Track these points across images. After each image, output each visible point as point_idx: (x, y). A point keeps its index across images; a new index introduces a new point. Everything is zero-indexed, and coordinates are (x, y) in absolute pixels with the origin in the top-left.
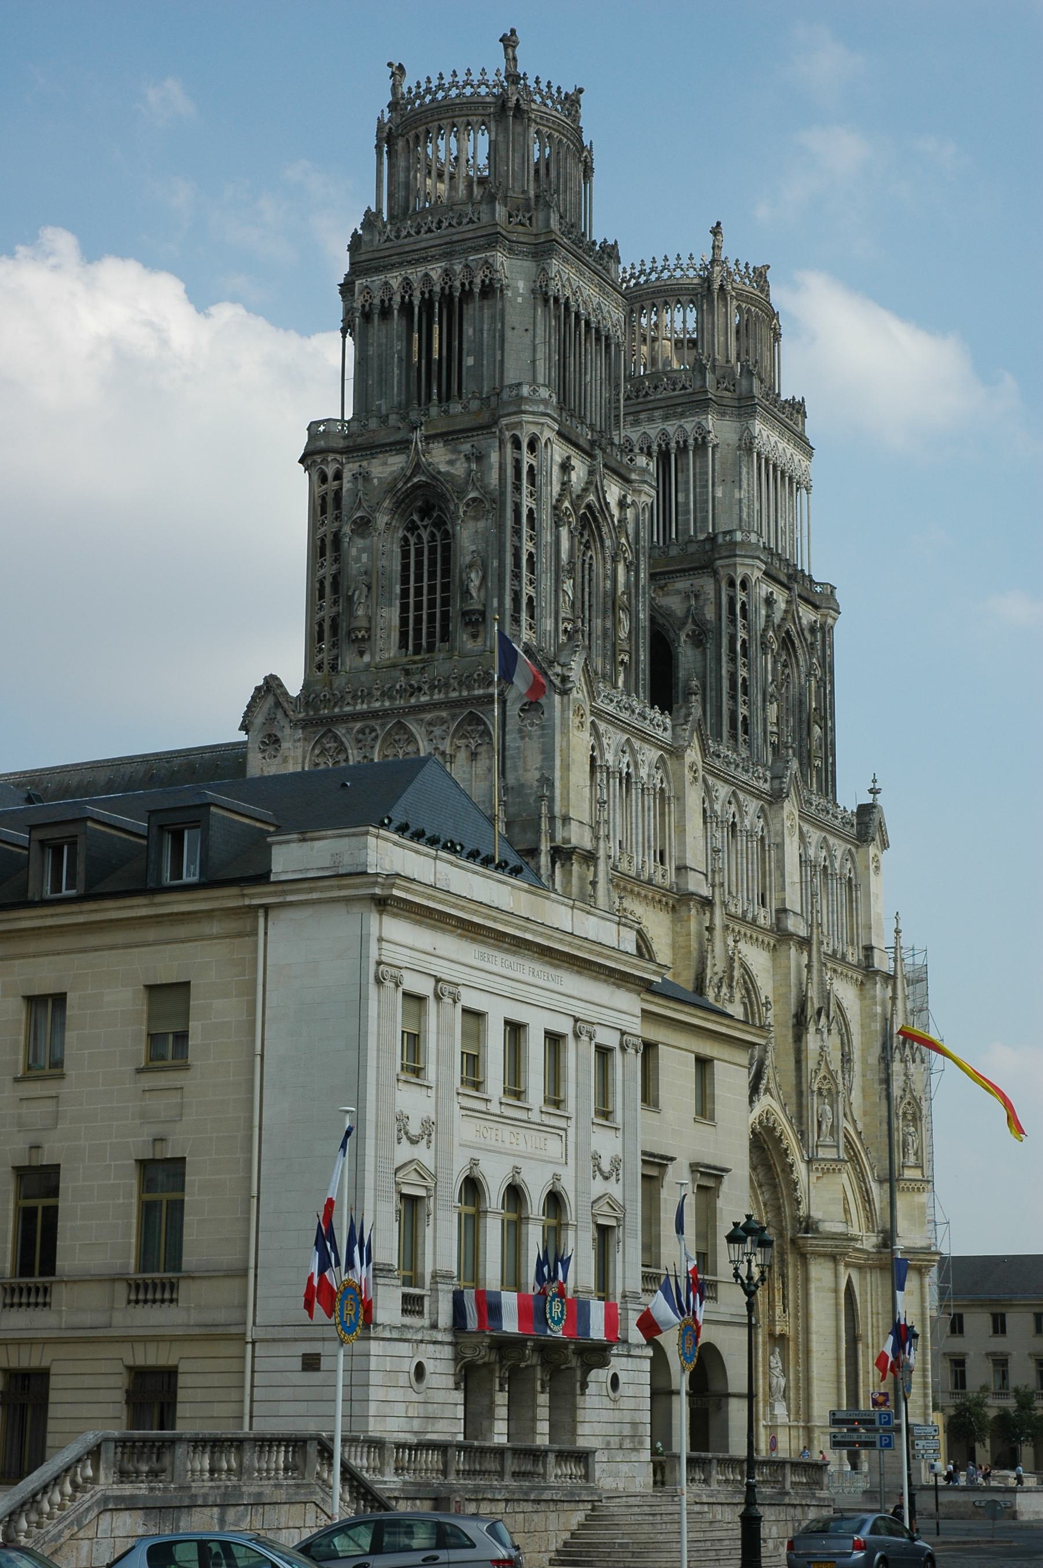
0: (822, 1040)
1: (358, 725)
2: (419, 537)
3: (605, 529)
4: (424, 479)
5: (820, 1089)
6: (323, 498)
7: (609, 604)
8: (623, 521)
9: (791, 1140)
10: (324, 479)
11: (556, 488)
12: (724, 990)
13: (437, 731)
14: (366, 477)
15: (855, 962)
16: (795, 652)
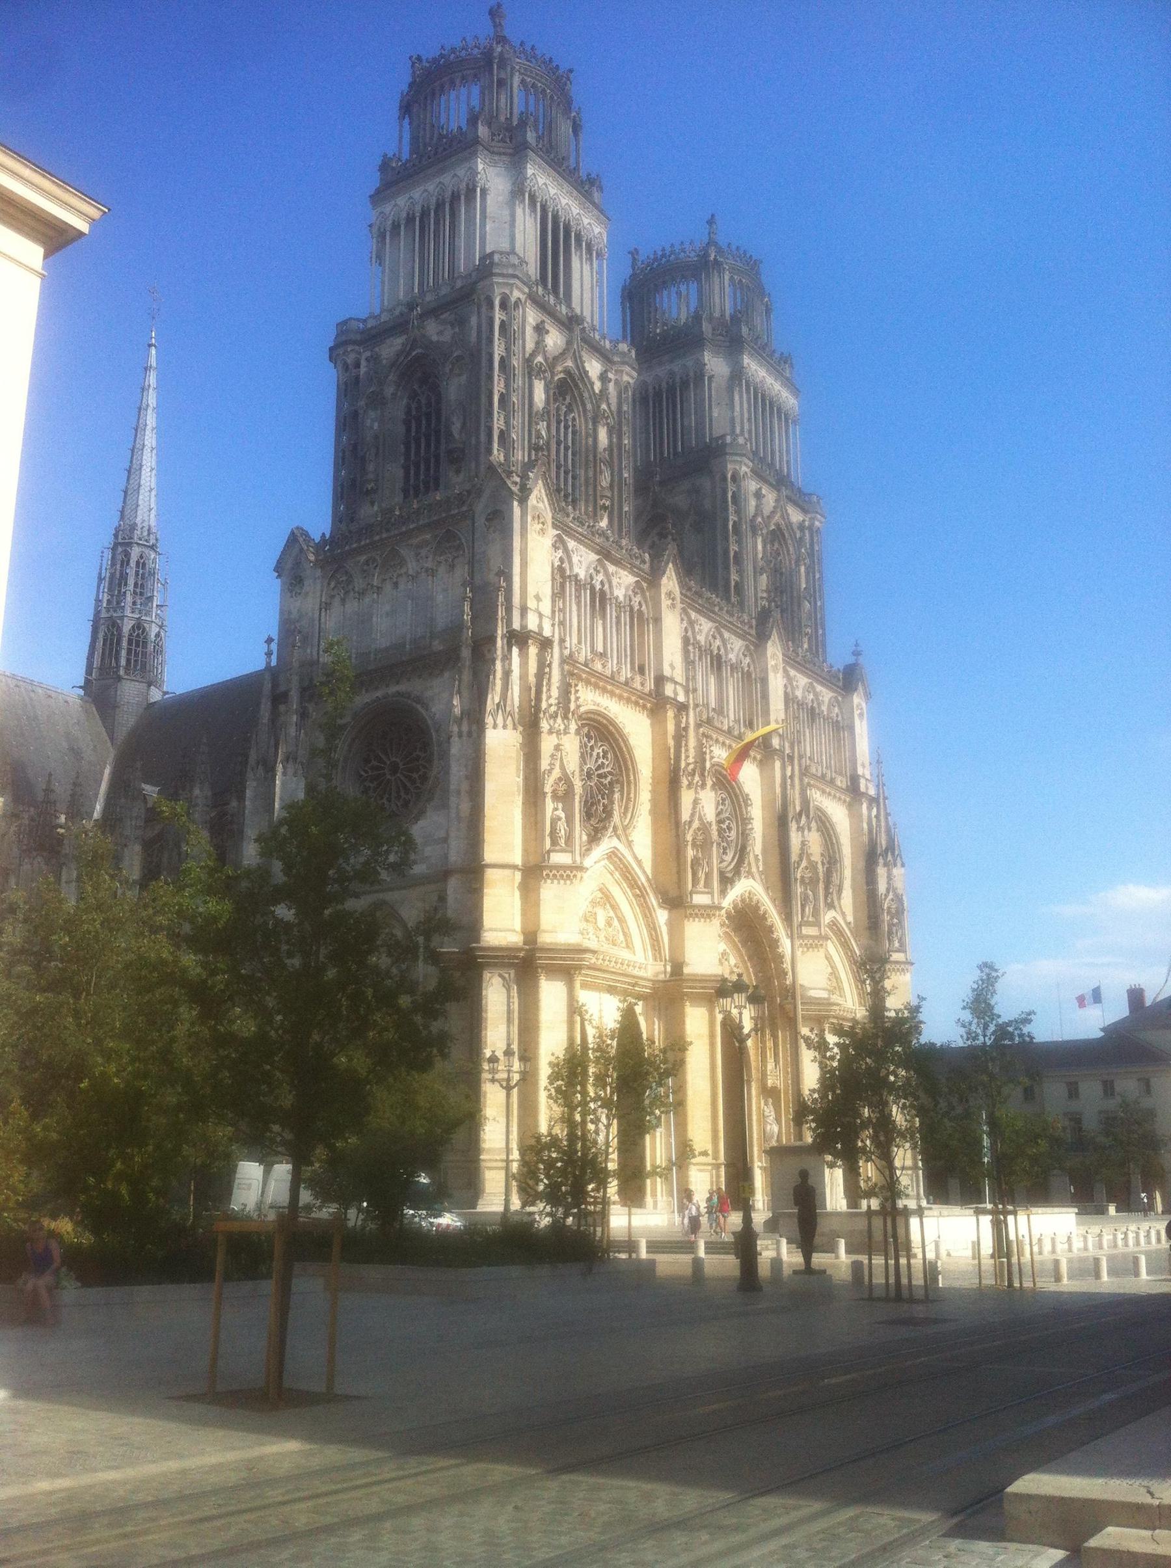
0: (803, 836)
1: (363, 558)
2: (419, 402)
3: (586, 395)
4: (420, 351)
5: (802, 877)
6: (346, 384)
7: (591, 458)
8: (604, 390)
9: (774, 917)
10: (346, 367)
11: (530, 346)
12: (697, 778)
13: (423, 552)
14: (374, 359)
15: (844, 786)
16: (786, 544)
